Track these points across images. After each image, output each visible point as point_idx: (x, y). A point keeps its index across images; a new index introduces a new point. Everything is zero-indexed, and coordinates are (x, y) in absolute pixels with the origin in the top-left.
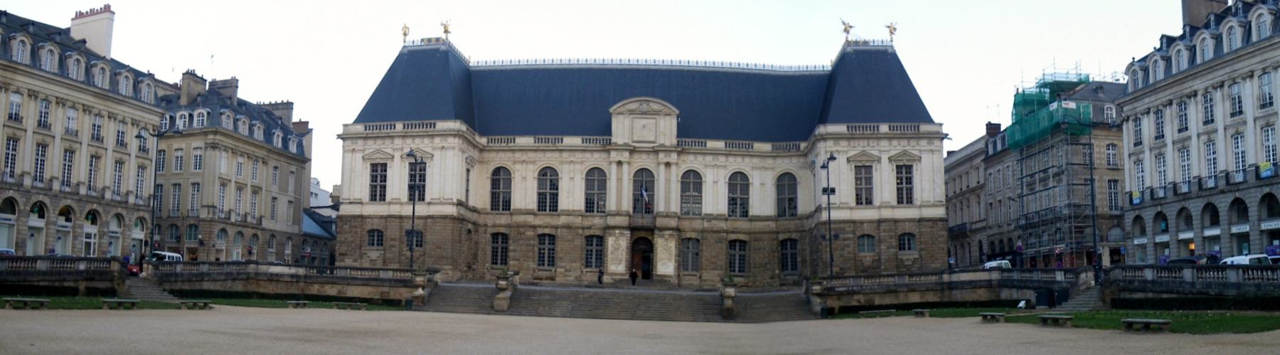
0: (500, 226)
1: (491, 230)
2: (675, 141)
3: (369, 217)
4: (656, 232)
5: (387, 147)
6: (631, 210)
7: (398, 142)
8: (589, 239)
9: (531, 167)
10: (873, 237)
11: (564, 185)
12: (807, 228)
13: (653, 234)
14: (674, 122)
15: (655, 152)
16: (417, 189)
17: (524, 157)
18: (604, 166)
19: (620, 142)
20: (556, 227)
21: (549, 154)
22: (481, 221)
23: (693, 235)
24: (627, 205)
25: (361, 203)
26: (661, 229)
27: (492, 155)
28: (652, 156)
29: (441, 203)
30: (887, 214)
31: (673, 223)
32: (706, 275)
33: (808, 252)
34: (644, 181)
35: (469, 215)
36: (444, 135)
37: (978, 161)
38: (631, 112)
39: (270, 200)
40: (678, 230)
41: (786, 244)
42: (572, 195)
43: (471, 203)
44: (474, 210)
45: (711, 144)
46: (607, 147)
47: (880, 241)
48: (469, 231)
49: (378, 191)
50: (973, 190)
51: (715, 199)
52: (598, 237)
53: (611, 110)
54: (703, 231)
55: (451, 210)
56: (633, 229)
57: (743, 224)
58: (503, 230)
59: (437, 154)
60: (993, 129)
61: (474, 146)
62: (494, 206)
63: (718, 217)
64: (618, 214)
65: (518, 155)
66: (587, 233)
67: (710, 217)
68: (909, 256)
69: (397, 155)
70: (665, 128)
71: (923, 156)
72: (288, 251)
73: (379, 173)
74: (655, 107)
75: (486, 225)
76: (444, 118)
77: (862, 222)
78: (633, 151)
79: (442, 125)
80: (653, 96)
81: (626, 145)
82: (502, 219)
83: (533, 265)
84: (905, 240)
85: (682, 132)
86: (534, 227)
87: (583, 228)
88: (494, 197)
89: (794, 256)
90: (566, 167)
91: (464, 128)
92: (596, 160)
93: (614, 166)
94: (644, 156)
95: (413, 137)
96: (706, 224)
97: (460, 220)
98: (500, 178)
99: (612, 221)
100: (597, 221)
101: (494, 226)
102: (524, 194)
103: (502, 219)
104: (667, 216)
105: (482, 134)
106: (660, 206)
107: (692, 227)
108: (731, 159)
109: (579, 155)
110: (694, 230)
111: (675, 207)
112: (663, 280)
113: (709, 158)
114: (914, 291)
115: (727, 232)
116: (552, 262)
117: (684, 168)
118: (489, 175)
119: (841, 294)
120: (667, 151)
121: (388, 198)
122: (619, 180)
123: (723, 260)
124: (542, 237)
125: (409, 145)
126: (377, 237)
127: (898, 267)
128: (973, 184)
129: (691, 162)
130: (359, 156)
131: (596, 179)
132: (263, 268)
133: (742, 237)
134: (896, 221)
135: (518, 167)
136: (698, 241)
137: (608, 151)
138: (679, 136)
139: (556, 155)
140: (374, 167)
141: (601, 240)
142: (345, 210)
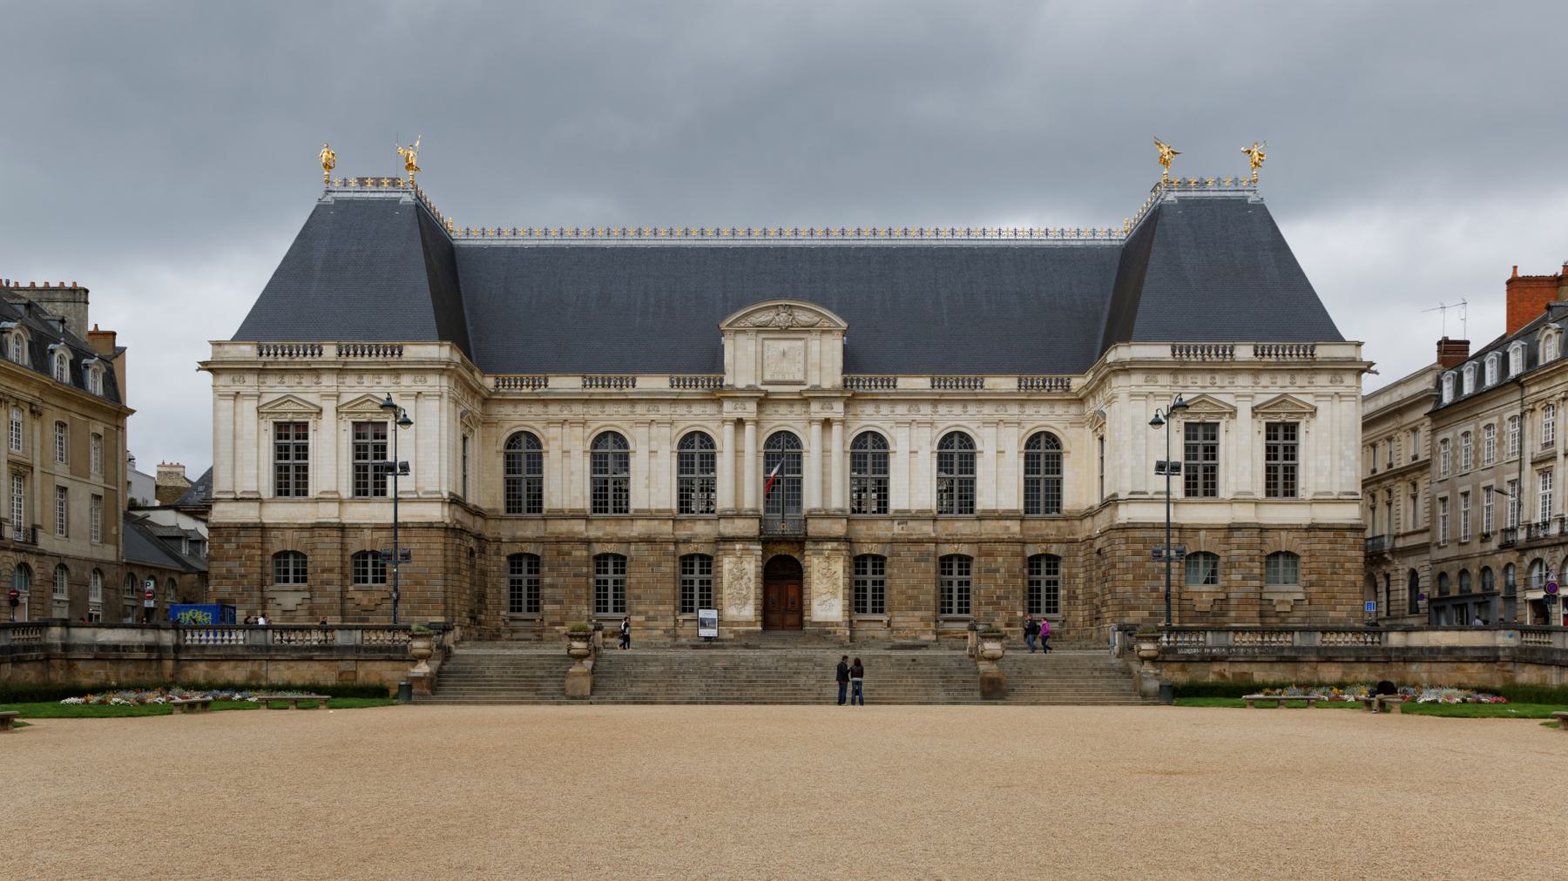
0: (526, 540)
1: (509, 550)
2: (838, 380)
3: (277, 527)
4: (809, 546)
5: (309, 391)
6: (761, 507)
7: (329, 382)
8: (687, 562)
9: (578, 430)
10: (1215, 557)
11: (638, 464)
12: (1080, 536)
13: (802, 550)
15: (805, 401)
17: (567, 413)
18: (711, 429)
19: (741, 383)
20: (628, 542)
21: (610, 409)
22: (488, 534)
23: (875, 549)
24: (752, 497)
25: (260, 500)
26: (818, 540)
27: (507, 410)
28: (798, 409)
29: (419, 500)
30: (1245, 514)
31: (839, 528)
32: (899, 620)
33: (1080, 580)
34: (782, 454)
35: (468, 521)
36: (421, 369)
37: (1420, 413)
38: (761, 329)
39: (51, 491)
40: (847, 540)
41: (1042, 565)
42: (653, 482)
43: (471, 500)
44: (476, 512)
45: (906, 383)
46: (718, 395)
47: (1231, 565)
48: (472, 553)
49: (291, 476)
50: (1402, 473)
51: (913, 483)
52: (702, 557)
53: (723, 326)
54: (894, 541)
55: (436, 513)
56: (766, 540)
58: (530, 549)
60: (1452, 352)
61: (474, 392)
62: (513, 504)
63: (919, 516)
64: (738, 514)
65: (553, 410)
66: (685, 550)
67: (905, 517)
68: (1285, 594)
69: (329, 406)
70: (820, 360)
71: (1320, 405)
72: (96, 598)
73: (291, 443)
74: (803, 317)
75: (499, 540)
76: (419, 338)
77: (1196, 529)
78: (764, 401)
79: (413, 352)
80: (795, 297)
81: (750, 388)
83: (585, 610)
84: (1280, 560)
85: (851, 363)
86: (588, 542)
87: (676, 543)
88: (511, 486)
89: (1053, 587)
91: (457, 358)
92: (699, 417)
93: (729, 429)
94: (783, 409)
95: (360, 372)
96: (897, 529)
97: (449, 530)
98: (523, 457)
99: (727, 528)
100: (702, 529)
101: (513, 541)
102: (567, 481)
104: (828, 516)
105: (485, 371)
106: (811, 499)
107: (874, 533)
108: (943, 409)
109: (665, 410)
110: (878, 541)
111: (839, 498)
112: (824, 633)
113: (901, 409)
114: (1330, 660)
115: (937, 542)
116: (620, 606)
117: (856, 428)
118: (501, 446)
119: (1189, 660)
120: (825, 397)
121: (313, 491)
122: (738, 453)
123: (929, 592)
124: (601, 560)
126: (291, 565)
127: (1262, 615)
128: (1404, 461)
129: (870, 418)
130: (249, 407)
131: (696, 455)
132: (82, 635)
133: (964, 550)
134: (1263, 529)
135: (554, 431)
136: (883, 558)
137: (719, 401)
138: (846, 370)
139: (624, 409)
140: (281, 429)
141: (707, 562)
142: (223, 513)
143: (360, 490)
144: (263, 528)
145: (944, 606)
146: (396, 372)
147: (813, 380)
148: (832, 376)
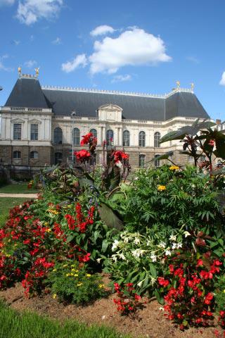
5: (22, 118)
7: (26, 116)
14: (120, 114)
16: (34, 136)
17: (67, 124)
19: (102, 120)
36: (46, 114)
38: (106, 110)
45: (133, 122)
46: (98, 123)
49: (17, 136)
51: (134, 141)
57: (144, 150)
59: (43, 122)
63: (136, 147)
65: (65, 124)
67: (132, 147)
69: (26, 121)
70: (117, 116)
73: (17, 127)
76: (45, 108)
78: (107, 123)
79: (44, 110)
82: (60, 147)
85: (123, 118)
90: (82, 128)
93: (100, 129)
103: (60, 147)
120: (119, 124)
121: (22, 139)
125: (31, 118)
143: (32, 138)
144: (12, 146)
145: (140, 165)
146: (40, 114)
147: (116, 120)
148: (120, 120)
